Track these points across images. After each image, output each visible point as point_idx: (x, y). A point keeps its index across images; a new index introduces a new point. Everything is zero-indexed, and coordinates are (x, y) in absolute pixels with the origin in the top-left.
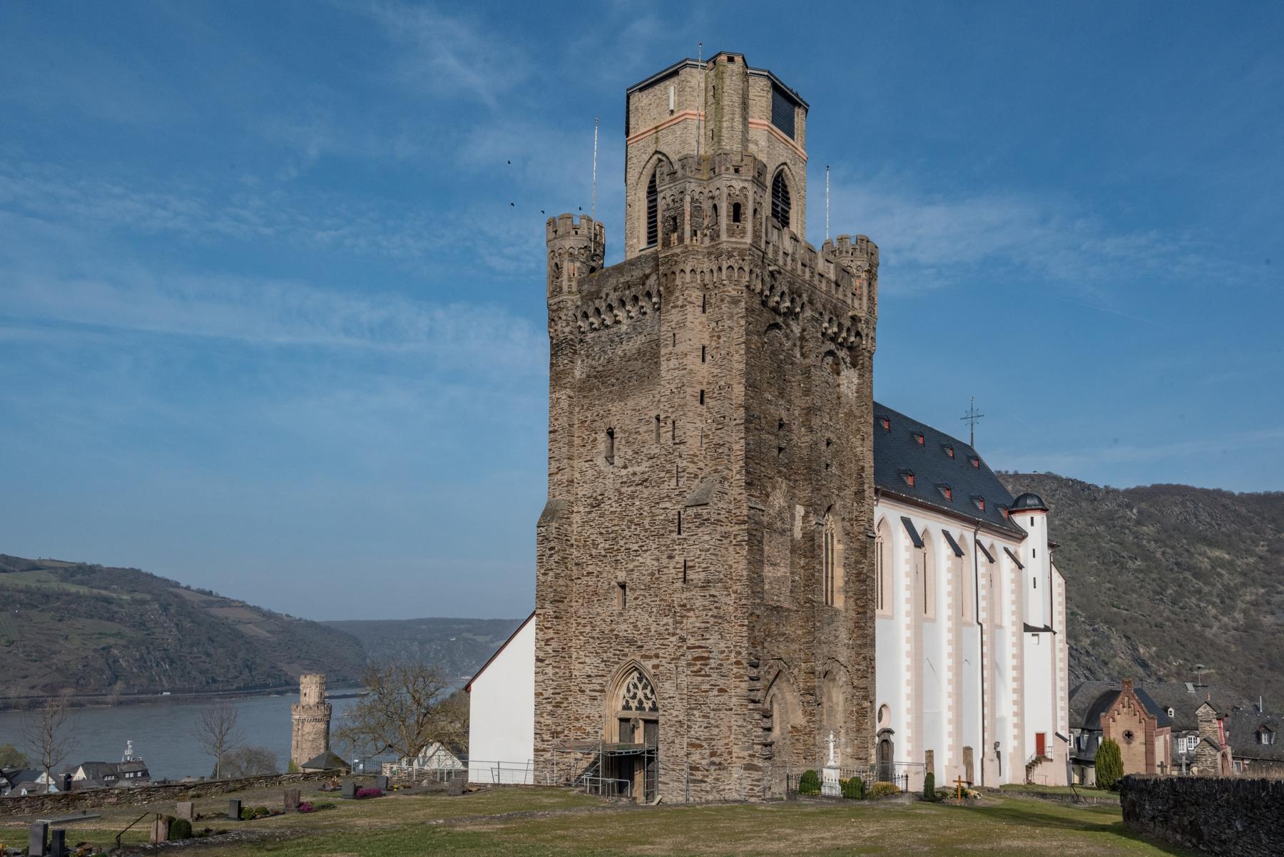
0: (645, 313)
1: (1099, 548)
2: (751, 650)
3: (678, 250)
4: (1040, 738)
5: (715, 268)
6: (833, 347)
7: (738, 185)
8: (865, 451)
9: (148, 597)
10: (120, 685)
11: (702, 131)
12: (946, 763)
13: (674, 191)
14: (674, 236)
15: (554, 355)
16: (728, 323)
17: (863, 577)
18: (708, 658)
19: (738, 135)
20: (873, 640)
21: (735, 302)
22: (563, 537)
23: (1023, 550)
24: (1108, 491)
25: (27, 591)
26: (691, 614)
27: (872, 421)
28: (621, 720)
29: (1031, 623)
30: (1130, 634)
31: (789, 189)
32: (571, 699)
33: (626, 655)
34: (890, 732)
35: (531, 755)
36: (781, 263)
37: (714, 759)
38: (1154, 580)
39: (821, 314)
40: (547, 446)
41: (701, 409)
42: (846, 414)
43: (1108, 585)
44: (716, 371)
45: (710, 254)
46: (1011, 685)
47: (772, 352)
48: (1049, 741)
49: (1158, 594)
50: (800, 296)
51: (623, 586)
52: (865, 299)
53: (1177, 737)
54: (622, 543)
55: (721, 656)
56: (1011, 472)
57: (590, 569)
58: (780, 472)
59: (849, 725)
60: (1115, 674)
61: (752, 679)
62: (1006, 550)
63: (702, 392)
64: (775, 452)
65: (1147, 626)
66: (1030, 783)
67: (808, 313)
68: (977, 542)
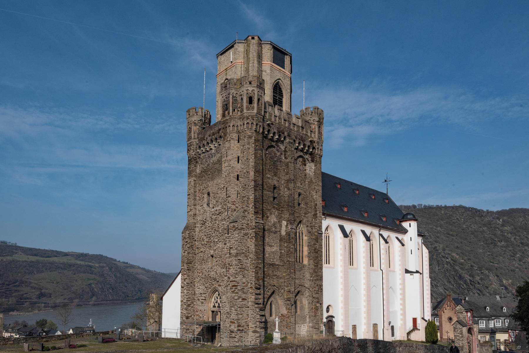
0: (220, 145)
1: (484, 237)
2: (256, 282)
3: (228, 118)
4: (415, 320)
5: (242, 124)
6: (302, 154)
7: (250, 89)
8: (317, 197)
9: (105, 265)
10: (94, 298)
11: (243, 69)
12: (363, 330)
13: (226, 94)
14: (227, 112)
15: (189, 164)
16: (247, 146)
17: (317, 250)
18: (237, 286)
19: (256, 69)
20: (322, 277)
21: (250, 137)
22: (191, 237)
23: (405, 238)
24: (488, 212)
25: (63, 264)
26: (231, 267)
27: (321, 184)
28: (213, 312)
29: (410, 270)
30: (498, 274)
31: (282, 90)
32: (195, 303)
33: (213, 285)
34: (333, 317)
35: (179, 326)
36: (273, 120)
37: (240, 328)
38: (510, 251)
39: (294, 141)
40: (186, 200)
41: (237, 182)
42: (309, 182)
43: (488, 253)
44: (243, 166)
45: (240, 118)
46: (399, 297)
47: (271, 157)
48: (419, 321)
49: (512, 257)
50: (283, 133)
51: (212, 256)
52: (317, 133)
53: (489, 320)
54: (212, 239)
55: (243, 285)
56: (443, 206)
57: (202, 250)
58: (274, 207)
59: (311, 314)
60: (492, 292)
61: (256, 294)
62: (397, 238)
63: (238, 175)
64: (272, 199)
65: (507, 271)
66: (409, 340)
67: (288, 140)
68: (381, 235)
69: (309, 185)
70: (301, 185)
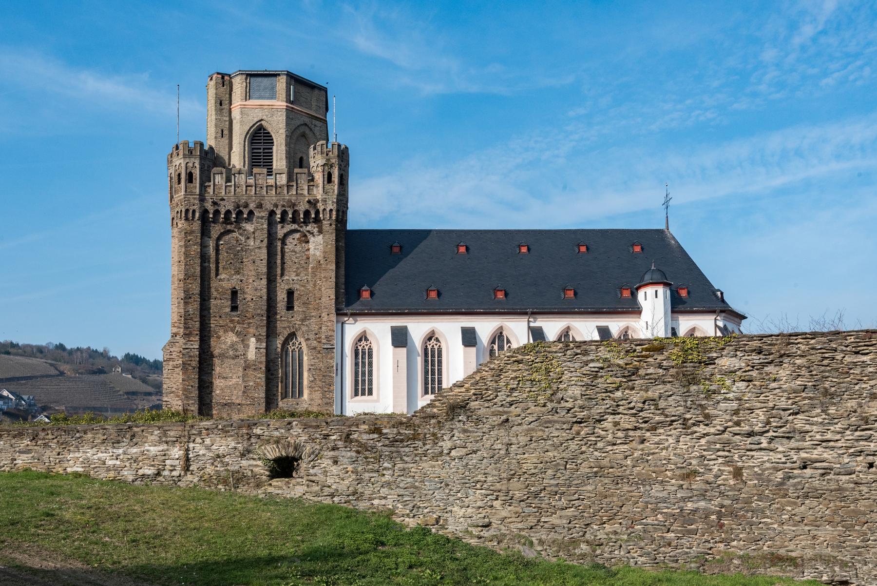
69: (313, 273)
70: (297, 275)
